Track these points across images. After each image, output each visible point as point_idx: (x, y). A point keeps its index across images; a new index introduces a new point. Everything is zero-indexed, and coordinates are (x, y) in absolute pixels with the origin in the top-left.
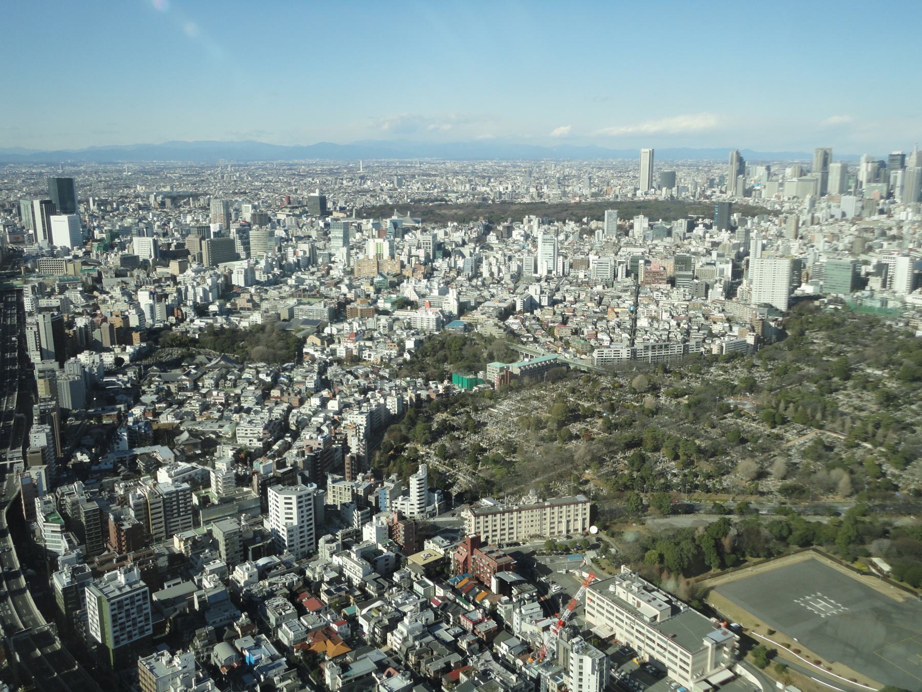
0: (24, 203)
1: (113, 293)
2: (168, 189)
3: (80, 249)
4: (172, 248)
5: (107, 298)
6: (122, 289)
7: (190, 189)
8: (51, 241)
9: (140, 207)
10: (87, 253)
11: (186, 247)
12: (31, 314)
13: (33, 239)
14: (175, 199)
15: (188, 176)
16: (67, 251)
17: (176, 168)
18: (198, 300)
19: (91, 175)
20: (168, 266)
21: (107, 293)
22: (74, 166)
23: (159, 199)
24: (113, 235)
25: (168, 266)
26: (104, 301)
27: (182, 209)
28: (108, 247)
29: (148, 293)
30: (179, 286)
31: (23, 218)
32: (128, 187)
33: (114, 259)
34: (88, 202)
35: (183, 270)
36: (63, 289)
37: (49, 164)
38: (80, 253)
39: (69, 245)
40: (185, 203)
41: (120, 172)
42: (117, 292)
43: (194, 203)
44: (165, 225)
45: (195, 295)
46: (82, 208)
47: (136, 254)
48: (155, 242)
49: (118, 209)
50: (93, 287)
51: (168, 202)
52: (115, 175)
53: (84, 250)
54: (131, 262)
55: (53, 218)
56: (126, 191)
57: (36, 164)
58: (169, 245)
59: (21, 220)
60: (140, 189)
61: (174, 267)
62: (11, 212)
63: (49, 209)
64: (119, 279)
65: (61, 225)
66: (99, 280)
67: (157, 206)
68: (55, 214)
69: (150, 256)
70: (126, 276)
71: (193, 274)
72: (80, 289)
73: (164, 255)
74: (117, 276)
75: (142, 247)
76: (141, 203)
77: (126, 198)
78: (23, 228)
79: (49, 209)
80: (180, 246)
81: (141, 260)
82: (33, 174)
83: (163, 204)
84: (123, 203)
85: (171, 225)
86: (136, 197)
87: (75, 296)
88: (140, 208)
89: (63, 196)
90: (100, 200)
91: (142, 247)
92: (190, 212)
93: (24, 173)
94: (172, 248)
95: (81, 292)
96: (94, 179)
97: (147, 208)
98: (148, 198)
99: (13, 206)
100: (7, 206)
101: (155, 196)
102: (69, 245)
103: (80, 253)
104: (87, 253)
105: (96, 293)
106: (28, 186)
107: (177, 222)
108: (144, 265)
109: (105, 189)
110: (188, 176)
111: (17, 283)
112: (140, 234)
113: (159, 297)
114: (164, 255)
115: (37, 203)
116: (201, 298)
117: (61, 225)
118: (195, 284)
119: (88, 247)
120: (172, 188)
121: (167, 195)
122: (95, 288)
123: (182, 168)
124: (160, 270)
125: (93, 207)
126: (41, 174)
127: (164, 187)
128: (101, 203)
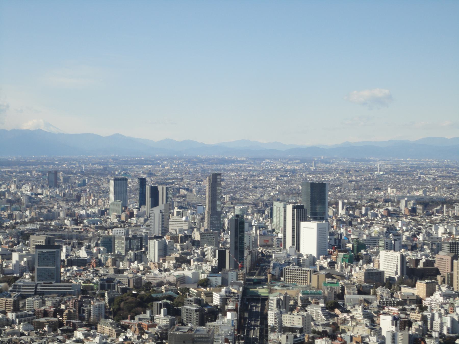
0: (277, 205)
1: (354, 313)
2: (420, 193)
3: (325, 258)
4: (421, 266)
5: (348, 318)
6: (364, 309)
7: (446, 195)
8: (298, 248)
9: (389, 214)
10: (332, 264)
11: (436, 265)
12: (273, 330)
13: (281, 243)
14: (428, 205)
15: (443, 177)
16: (312, 261)
17: (430, 168)
18: (445, 332)
19: (342, 174)
20: (413, 286)
21: (348, 312)
22: (326, 163)
23: (411, 204)
24: (360, 246)
25: (413, 286)
26: (345, 321)
27: (434, 217)
28: (354, 259)
29: (390, 318)
30: (425, 313)
31: (275, 220)
32: (379, 189)
33: (358, 273)
34: (337, 204)
35: (430, 293)
36: (306, 303)
37: (303, 161)
38: (325, 264)
39: (315, 254)
40: (438, 211)
41: (372, 170)
42: (358, 312)
43: (448, 212)
44: (414, 236)
45: (442, 325)
46: (330, 213)
47: (381, 269)
48: (403, 257)
49: (366, 214)
50: (335, 303)
51: (420, 208)
52: (367, 175)
53: (329, 260)
54: (375, 278)
55: (303, 224)
56: (376, 193)
57: (291, 160)
58: (417, 261)
59: (272, 221)
60: (391, 192)
61: (420, 289)
62: (264, 212)
63: (301, 214)
64: (362, 297)
65: (310, 231)
66: (341, 296)
67: (407, 213)
68: (305, 220)
69: (396, 273)
70: (368, 294)
71: (441, 299)
72: (322, 305)
73: (411, 274)
74: (360, 293)
75: (388, 262)
76: (390, 208)
77: (376, 201)
78: (274, 230)
79: (301, 214)
80: (429, 263)
81: (386, 276)
82: (286, 171)
83: (413, 211)
84: (372, 207)
85: (421, 237)
86: (386, 201)
87: (316, 311)
88: (389, 214)
89: (315, 202)
90: (350, 203)
91: (388, 262)
92: (442, 221)
93: (278, 170)
94: (421, 266)
95: (323, 309)
96: (345, 178)
97: (395, 214)
98: (398, 202)
99: (266, 206)
100: (261, 205)
101: (406, 202)
102: (315, 254)
103: (325, 264)
104: (332, 264)
105: (337, 311)
106: (281, 184)
107: (428, 234)
108: (390, 283)
109: (355, 190)
110: (443, 177)
111: (262, 291)
112: (389, 247)
113: (403, 324)
114: (411, 274)
115: (289, 208)
116: (448, 329)
117: (310, 231)
118: (443, 311)
119: (333, 257)
120: (424, 192)
121: (419, 201)
122: (337, 306)
123: (437, 168)
124: (406, 290)
125: (341, 211)
126: (294, 172)
127: (416, 190)
128: (351, 206)
